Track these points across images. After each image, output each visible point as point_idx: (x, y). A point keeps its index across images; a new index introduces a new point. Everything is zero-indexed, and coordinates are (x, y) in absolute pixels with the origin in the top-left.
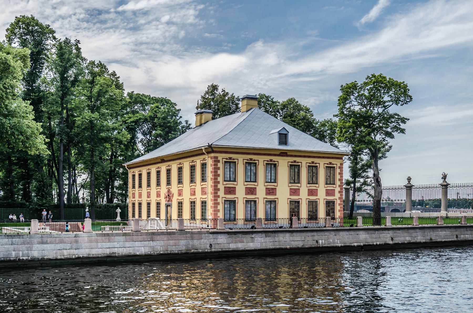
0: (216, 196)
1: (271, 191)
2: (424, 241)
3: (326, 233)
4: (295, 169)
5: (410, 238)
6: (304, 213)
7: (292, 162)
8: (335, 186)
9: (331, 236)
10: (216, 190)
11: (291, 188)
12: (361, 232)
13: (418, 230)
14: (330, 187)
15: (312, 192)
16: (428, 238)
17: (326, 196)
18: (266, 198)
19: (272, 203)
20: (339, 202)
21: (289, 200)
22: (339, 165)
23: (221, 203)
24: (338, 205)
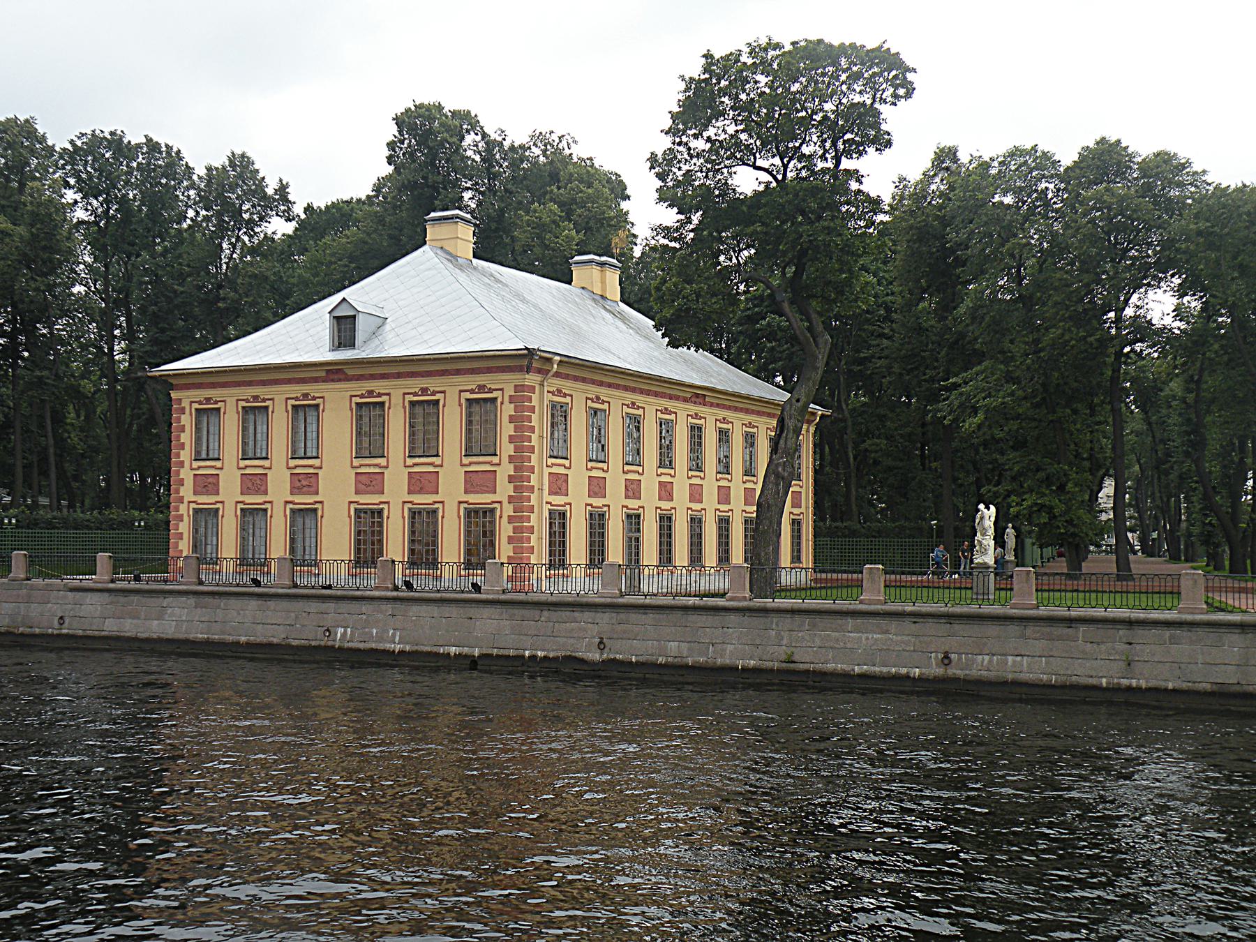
1: (304, 483)
3: (365, 607)
4: (369, 416)
6: (396, 545)
7: (362, 396)
8: (495, 460)
9: (380, 616)
11: (359, 471)
12: (487, 611)
13: (733, 618)
15: (420, 483)
16: (781, 653)
19: (304, 517)
20: (508, 510)
21: (353, 506)
22: (510, 391)
23: (186, 518)
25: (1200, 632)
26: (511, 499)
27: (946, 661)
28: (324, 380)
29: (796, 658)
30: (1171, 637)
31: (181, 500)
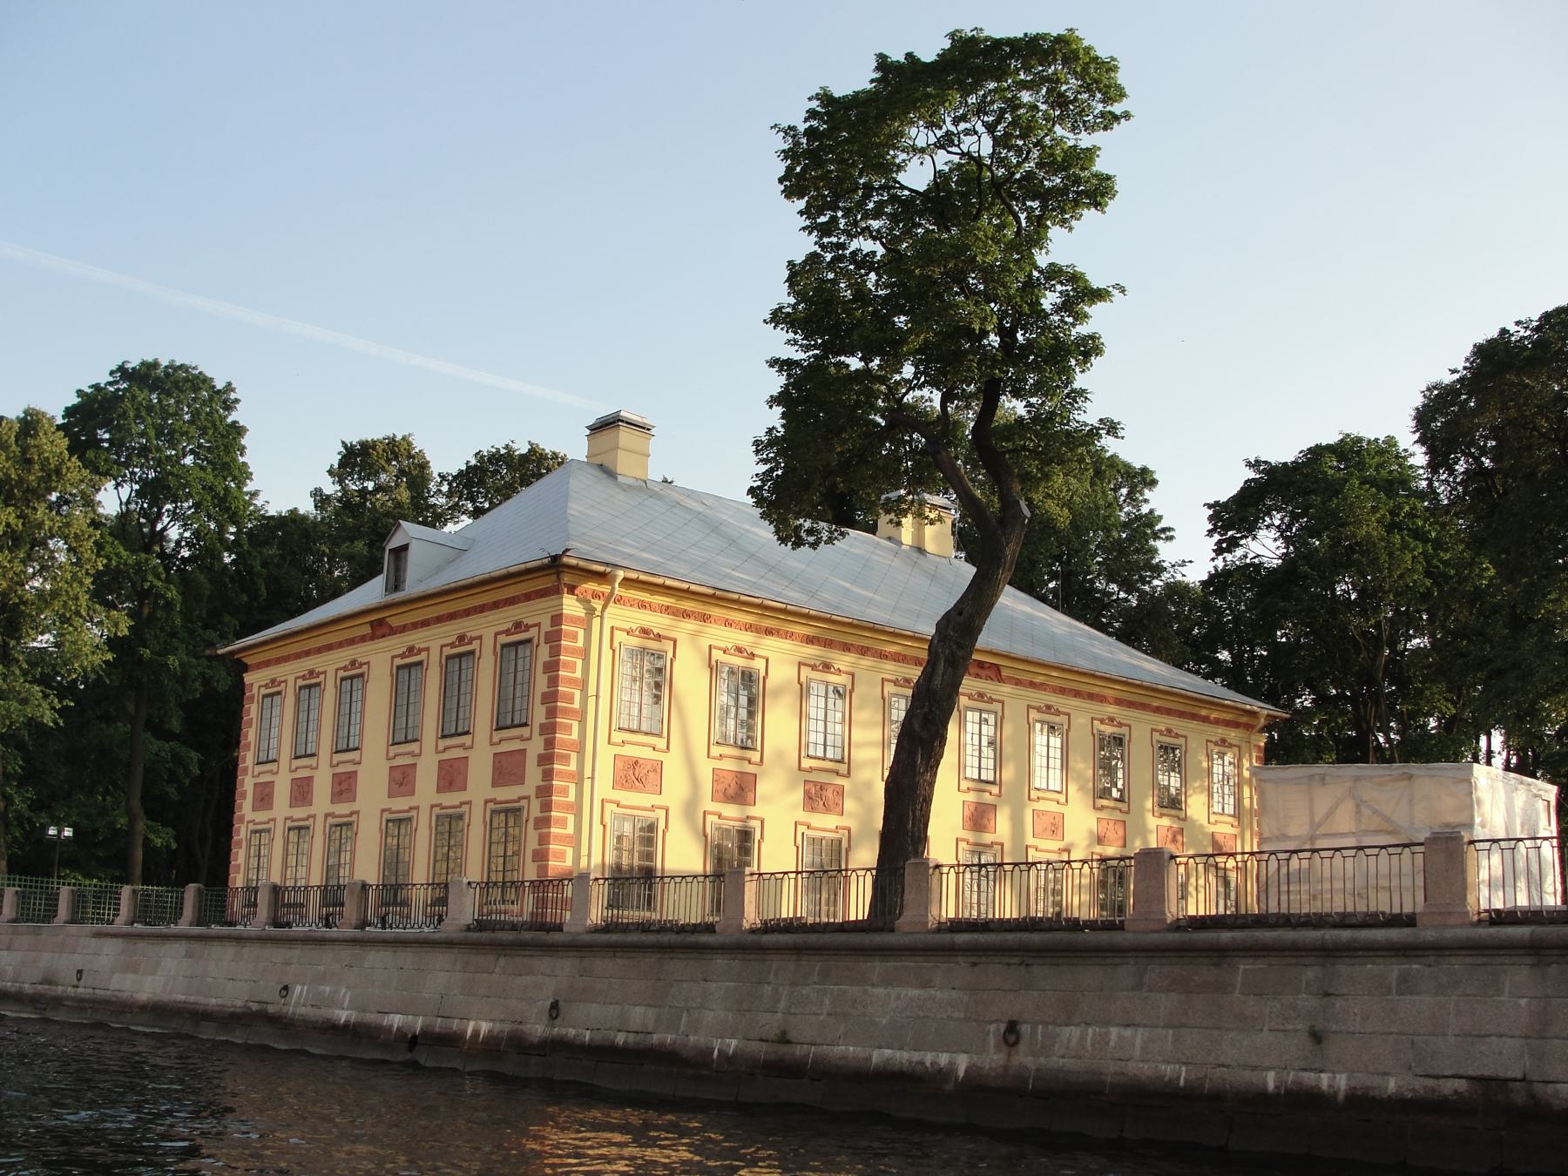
2: (733, 1044)
5: (651, 1013)
8: (525, 731)
13: (721, 962)
16: (771, 1023)
17: (494, 784)
25: (1456, 965)
27: (1012, 1039)
28: (373, 637)
29: (792, 1035)
30: (1403, 978)
31: (242, 819)
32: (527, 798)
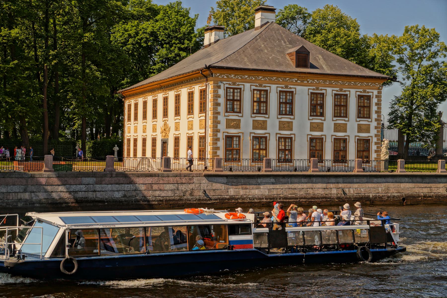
0: (216, 131)
8: (370, 120)
10: (216, 122)
14: (364, 122)
17: (358, 132)
18: (280, 134)
20: (375, 140)
24: (373, 143)
26: (376, 136)
32: (372, 137)
